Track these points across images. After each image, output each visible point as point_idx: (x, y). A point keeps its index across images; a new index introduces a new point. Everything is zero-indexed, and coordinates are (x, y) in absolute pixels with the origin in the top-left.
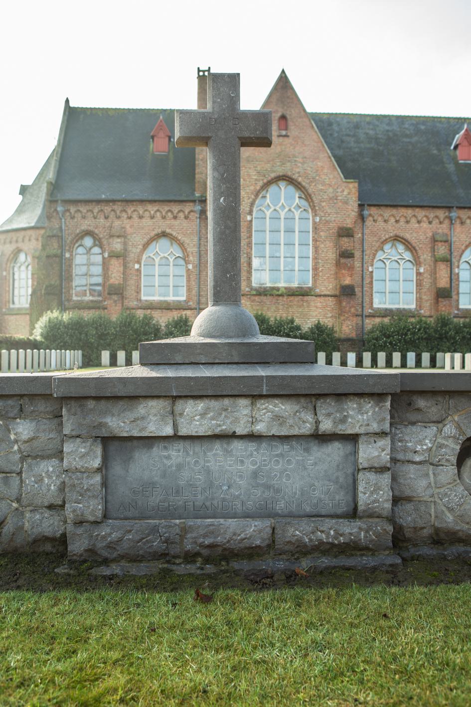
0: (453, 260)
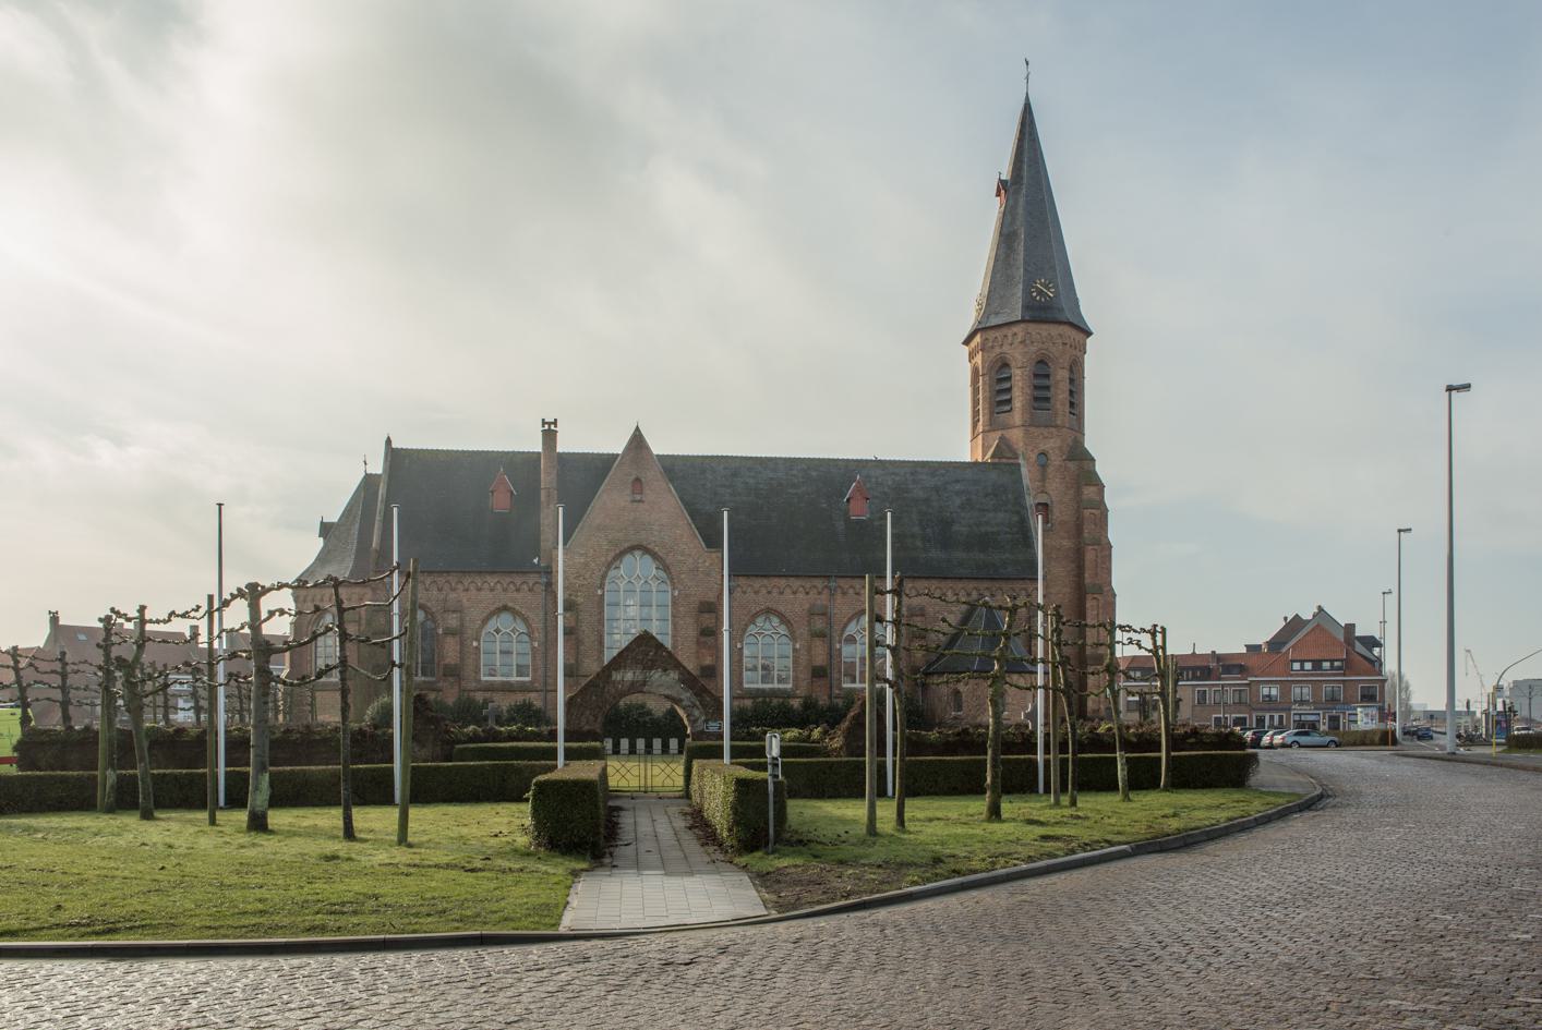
0: (834, 634)
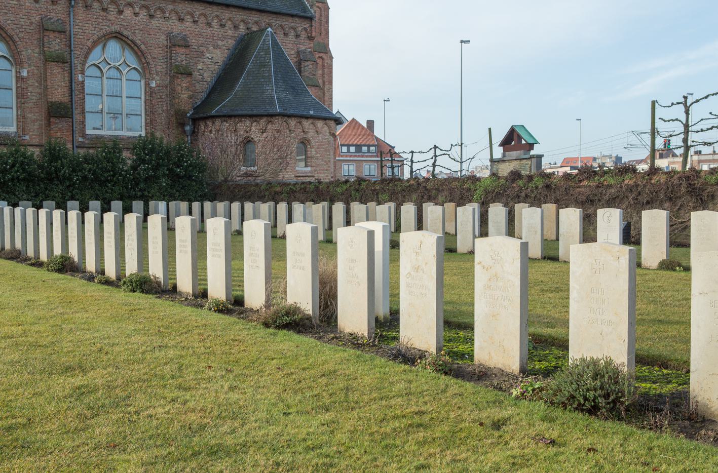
0: (74, 61)
